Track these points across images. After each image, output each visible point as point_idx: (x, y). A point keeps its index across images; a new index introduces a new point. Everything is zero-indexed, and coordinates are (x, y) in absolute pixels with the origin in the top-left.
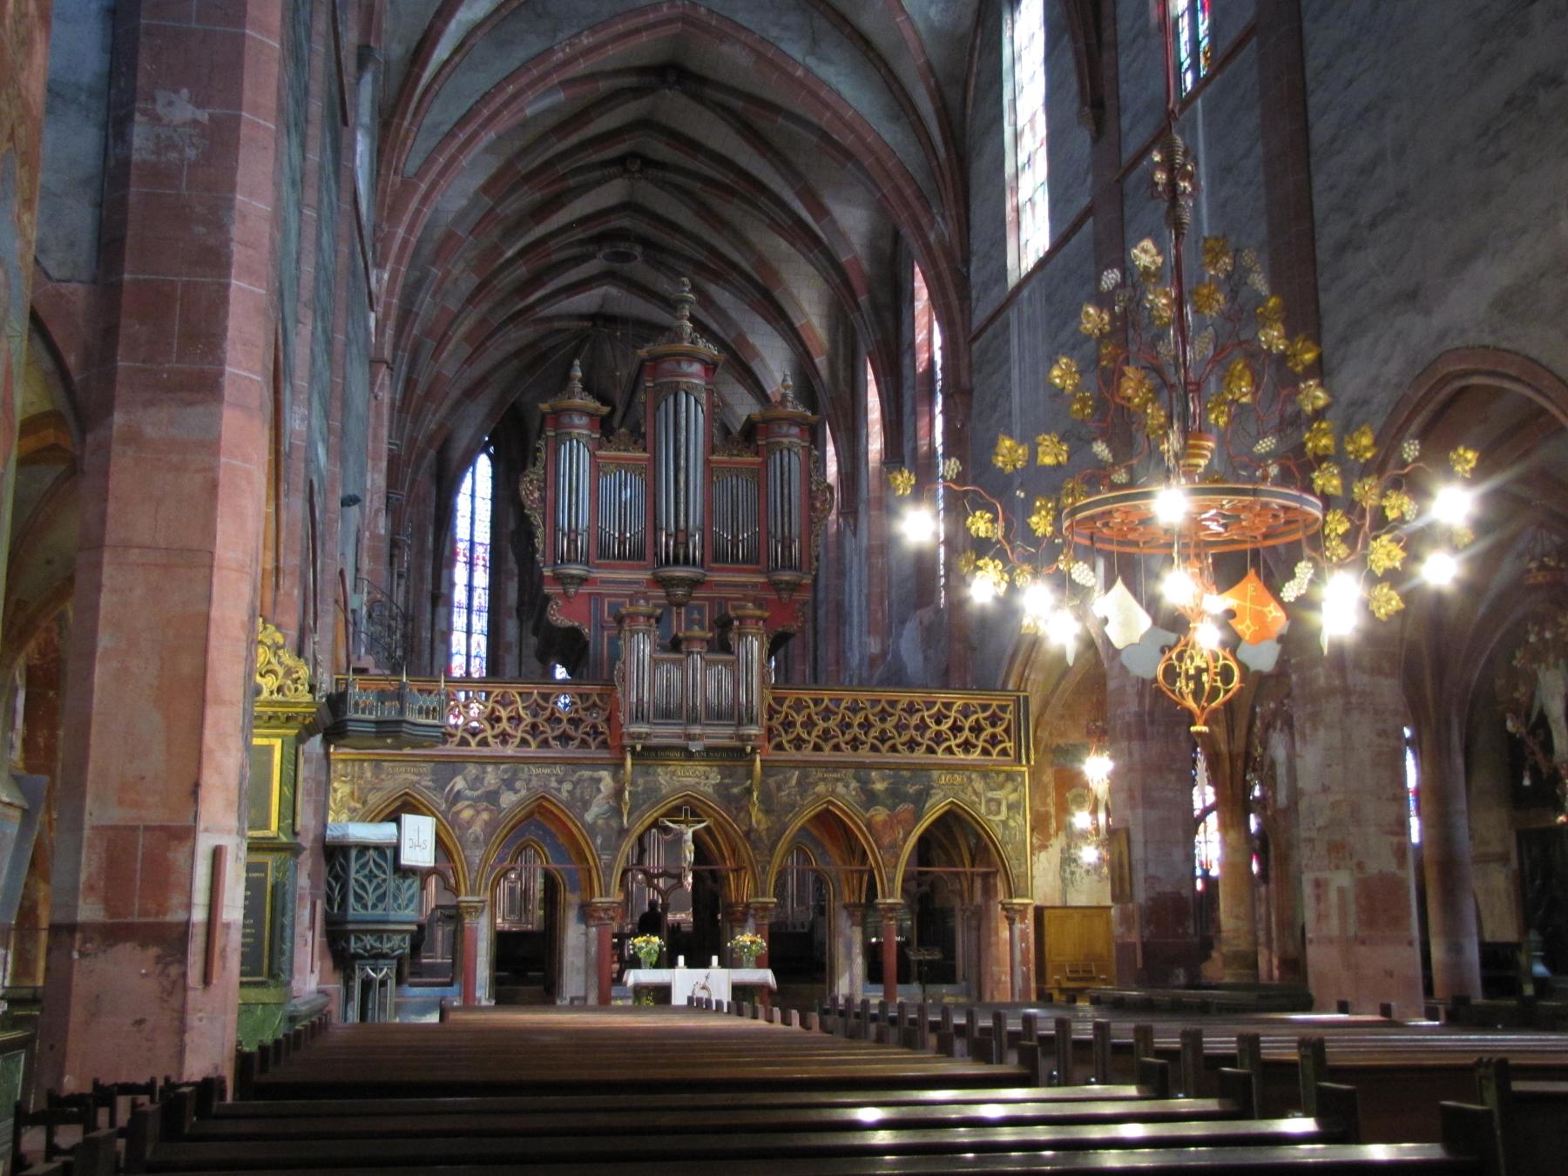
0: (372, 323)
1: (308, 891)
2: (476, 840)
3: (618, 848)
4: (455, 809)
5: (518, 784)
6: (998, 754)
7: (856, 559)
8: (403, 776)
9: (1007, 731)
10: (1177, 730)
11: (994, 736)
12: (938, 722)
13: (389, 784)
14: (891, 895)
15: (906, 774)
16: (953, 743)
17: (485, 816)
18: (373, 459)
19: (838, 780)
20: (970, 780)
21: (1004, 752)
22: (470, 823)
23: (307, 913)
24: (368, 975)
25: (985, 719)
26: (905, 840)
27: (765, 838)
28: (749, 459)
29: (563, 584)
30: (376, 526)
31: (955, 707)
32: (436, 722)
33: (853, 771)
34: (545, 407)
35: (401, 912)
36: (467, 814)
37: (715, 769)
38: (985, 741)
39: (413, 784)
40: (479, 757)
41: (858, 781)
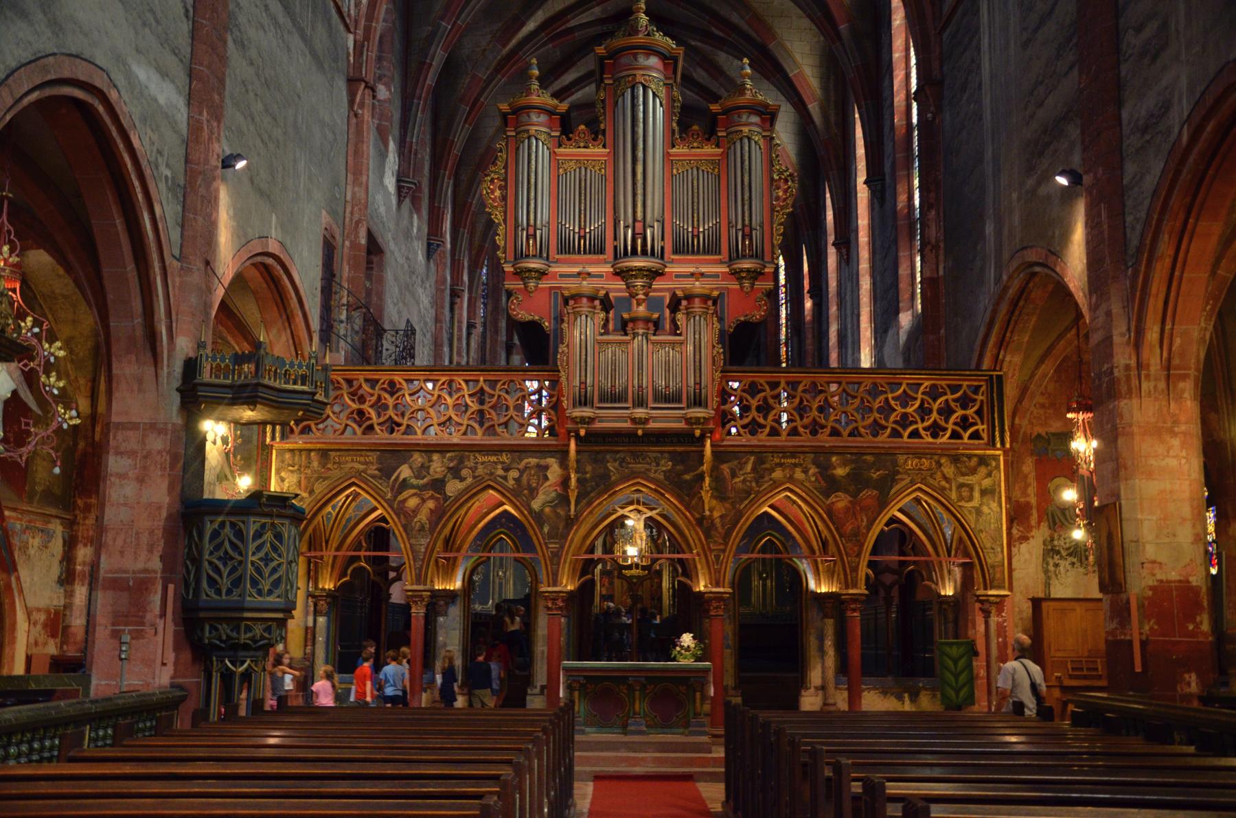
0: (351, 44)
1: (159, 575)
2: (422, 528)
3: (566, 539)
4: (400, 498)
5: (464, 472)
6: (971, 437)
7: (849, 285)
8: (349, 465)
9: (979, 413)
10: (1181, 385)
11: (964, 418)
12: (904, 405)
13: (336, 473)
14: (855, 586)
15: (869, 458)
16: (920, 426)
17: (431, 504)
18: (354, 174)
19: (795, 465)
20: (939, 465)
21: (976, 436)
22: (416, 511)
23: (157, 599)
24: (228, 668)
25: (954, 400)
26: (869, 528)
27: (719, 525)
28: (709, 150)
29: (523, 279)
30: (357, 236)
31: (922, 389)
32: (305, 388)
33: (812, 456)
34: (504, 107)
35: (260, 599)
36: (412, 503)
37: (666, 455)
38: (955, 424)
39: (359, 474)
40: (424, 445)
41: (818, 467)
